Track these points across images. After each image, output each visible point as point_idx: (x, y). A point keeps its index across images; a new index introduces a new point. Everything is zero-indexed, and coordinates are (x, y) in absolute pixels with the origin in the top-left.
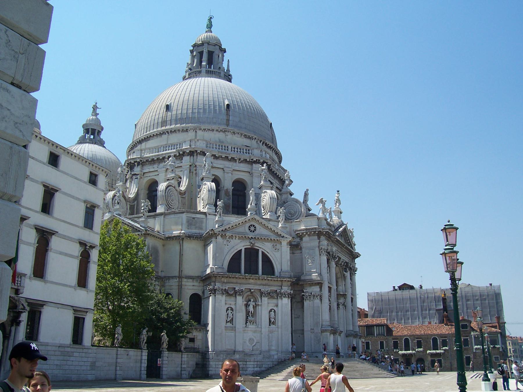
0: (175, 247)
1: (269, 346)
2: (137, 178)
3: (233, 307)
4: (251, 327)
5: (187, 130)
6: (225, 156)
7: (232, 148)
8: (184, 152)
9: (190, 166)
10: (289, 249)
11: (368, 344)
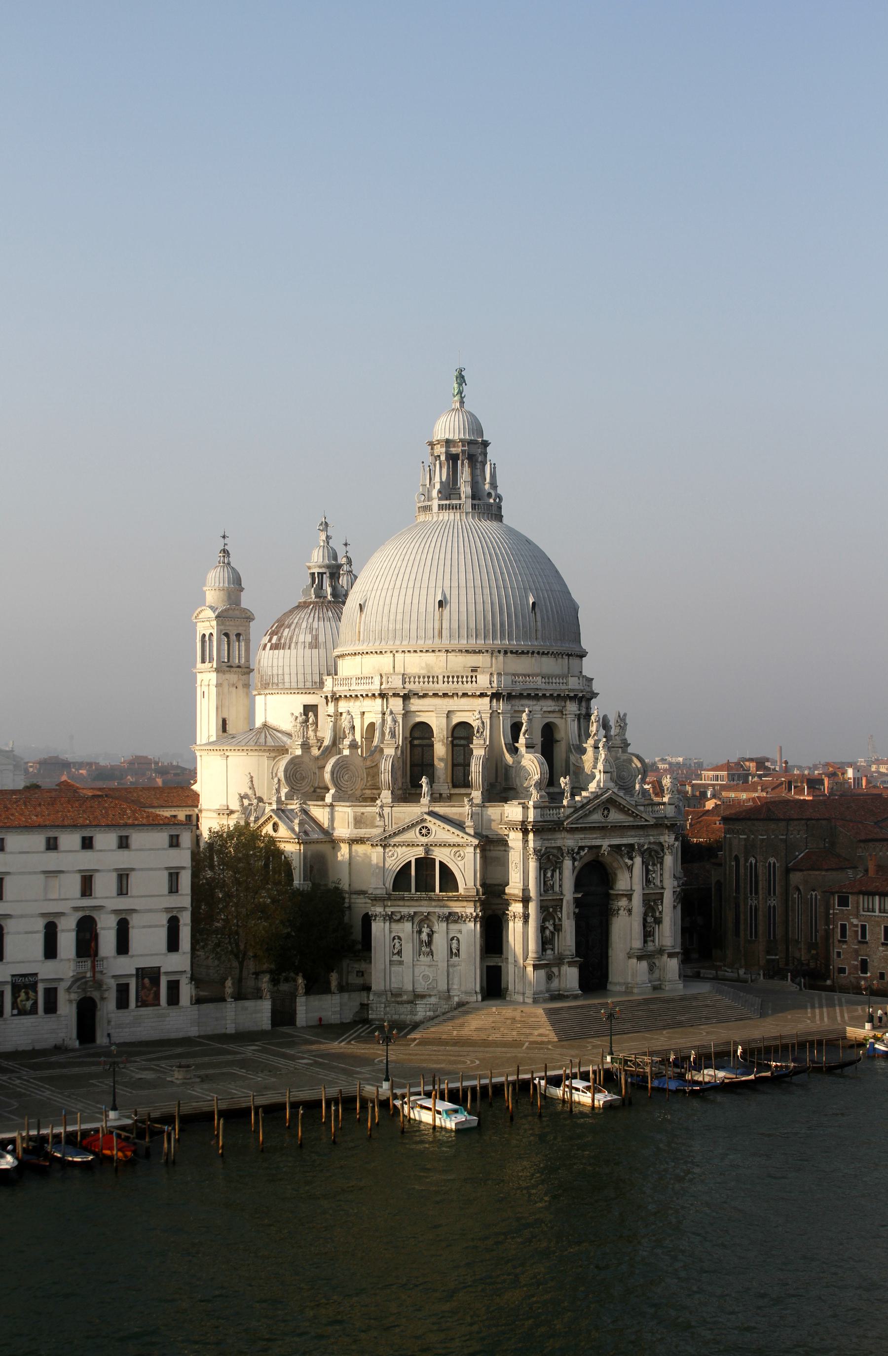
6: (434, 694)
7: (444, 677)
8: (374, 695)
11: (863, 927)
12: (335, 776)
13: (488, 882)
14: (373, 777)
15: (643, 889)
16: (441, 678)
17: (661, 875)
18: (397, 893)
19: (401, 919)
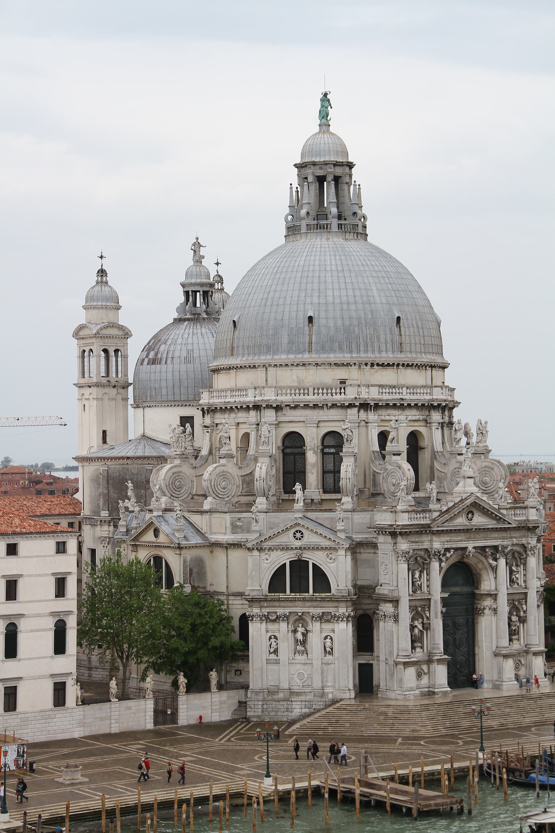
0: (220, 555)
1: (322, 681)
2: (208, 432)
4: (300, 658)
7: (314, 389)
8: (248, 406)
10: (349, 558)
12: (212, 483)
13: (359, 583)
14: (248, 484)
15: (507, 589)
16: (311, 390)
17: (525, 575)
18: (273, 594)
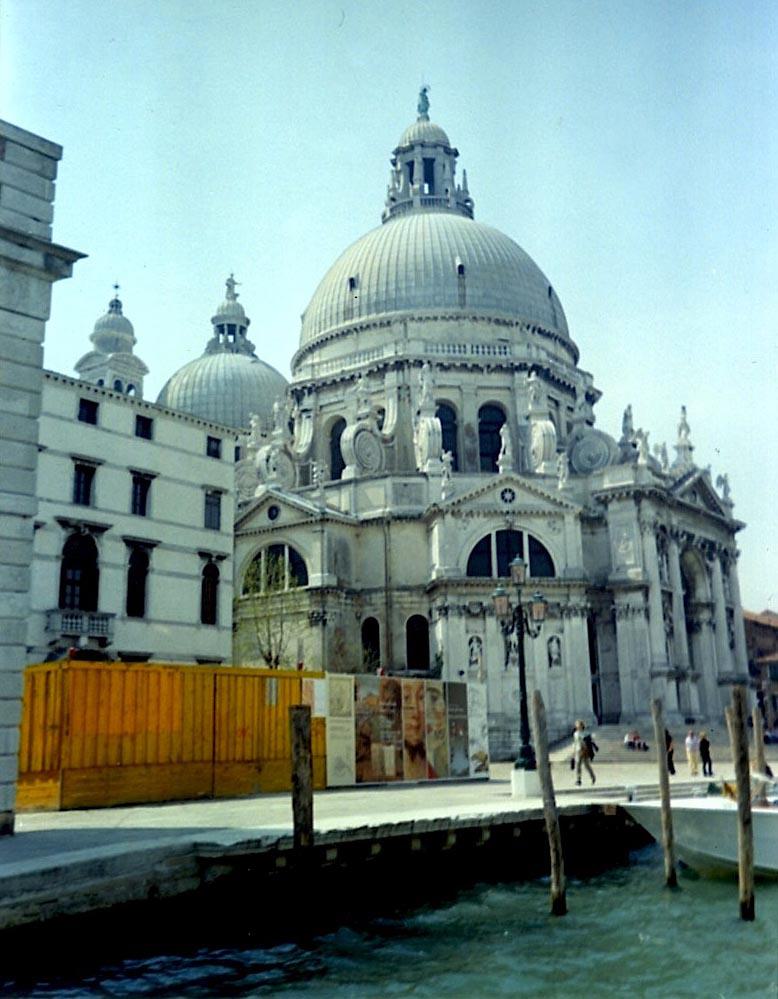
0: (374, 536)
2: (309, 417)
3: (481, 636)
5: (389, 323)
8: (386, 365)
9: (399, 388)
16: (469, 347)
19: (484, 612)
